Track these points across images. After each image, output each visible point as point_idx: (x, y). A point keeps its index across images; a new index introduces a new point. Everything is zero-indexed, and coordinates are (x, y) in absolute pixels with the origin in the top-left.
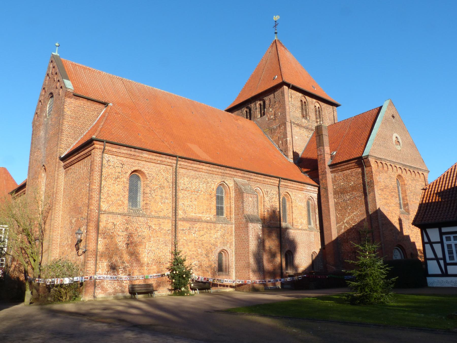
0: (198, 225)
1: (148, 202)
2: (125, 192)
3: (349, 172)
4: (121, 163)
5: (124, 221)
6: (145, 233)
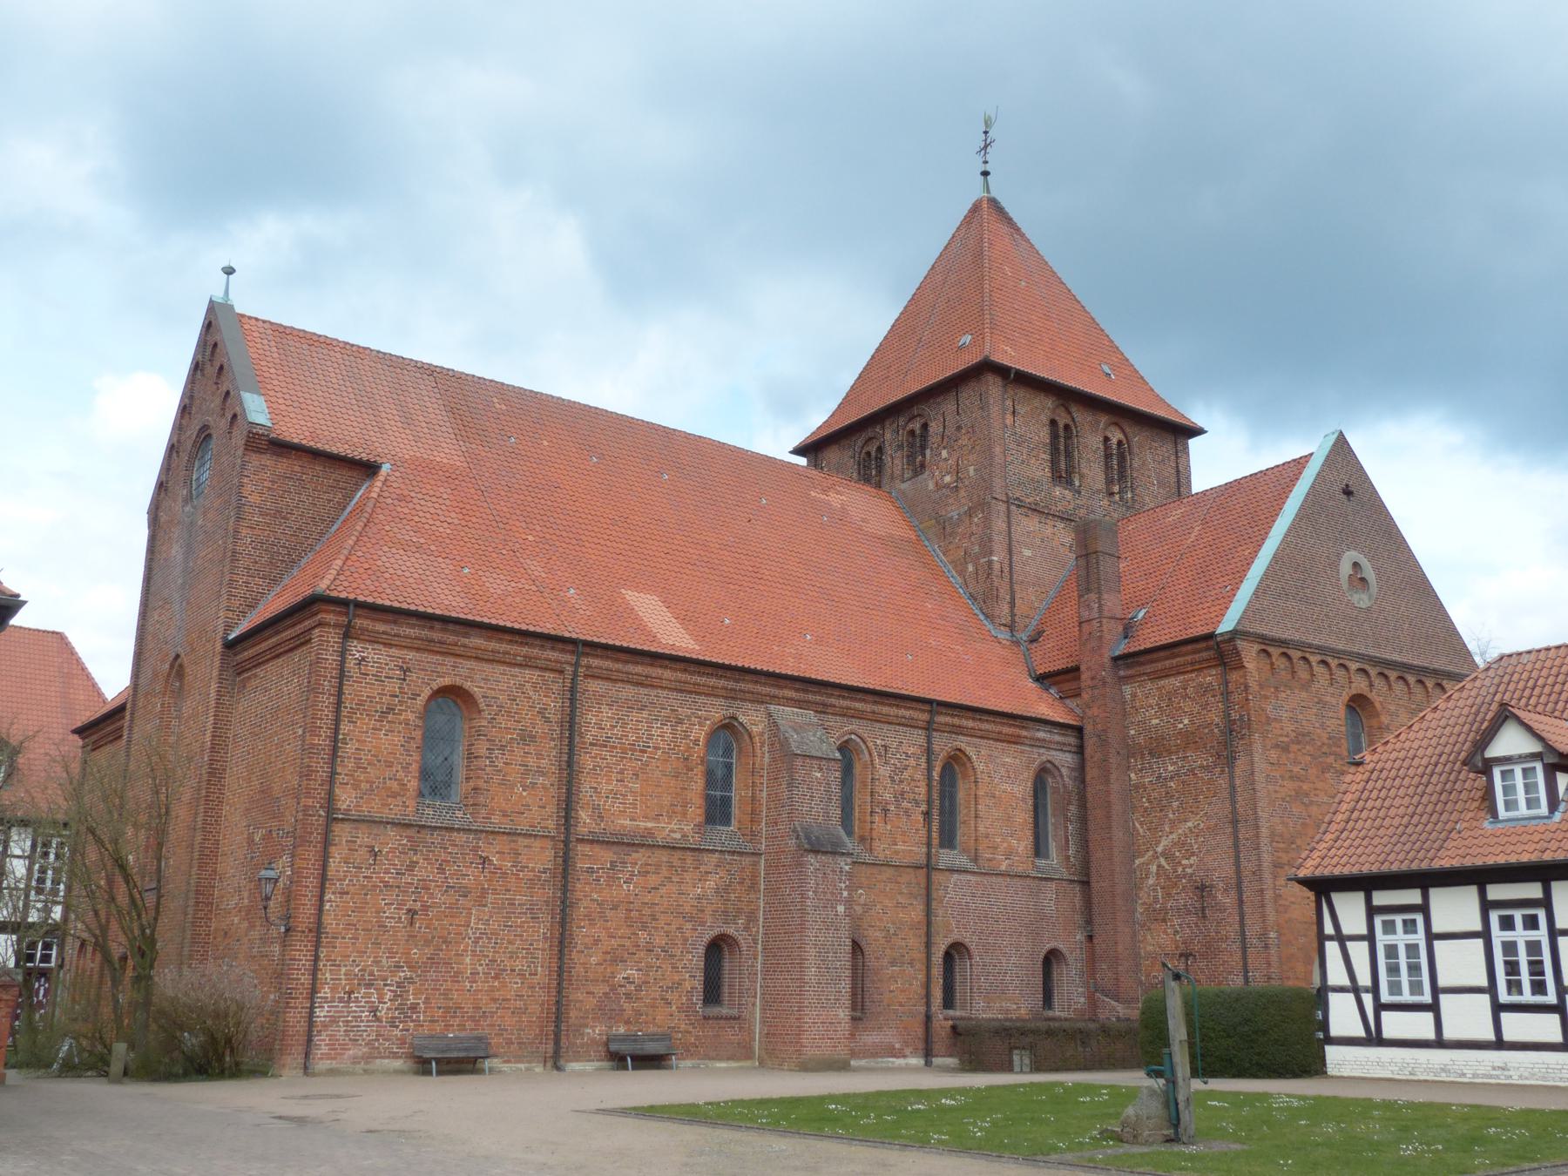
0: (640, 856)
1: (481, 783)
2: (411, 756)
3: (1175, 682)
4: (402, 667)
5: (405, 842)
6: (469, 880)
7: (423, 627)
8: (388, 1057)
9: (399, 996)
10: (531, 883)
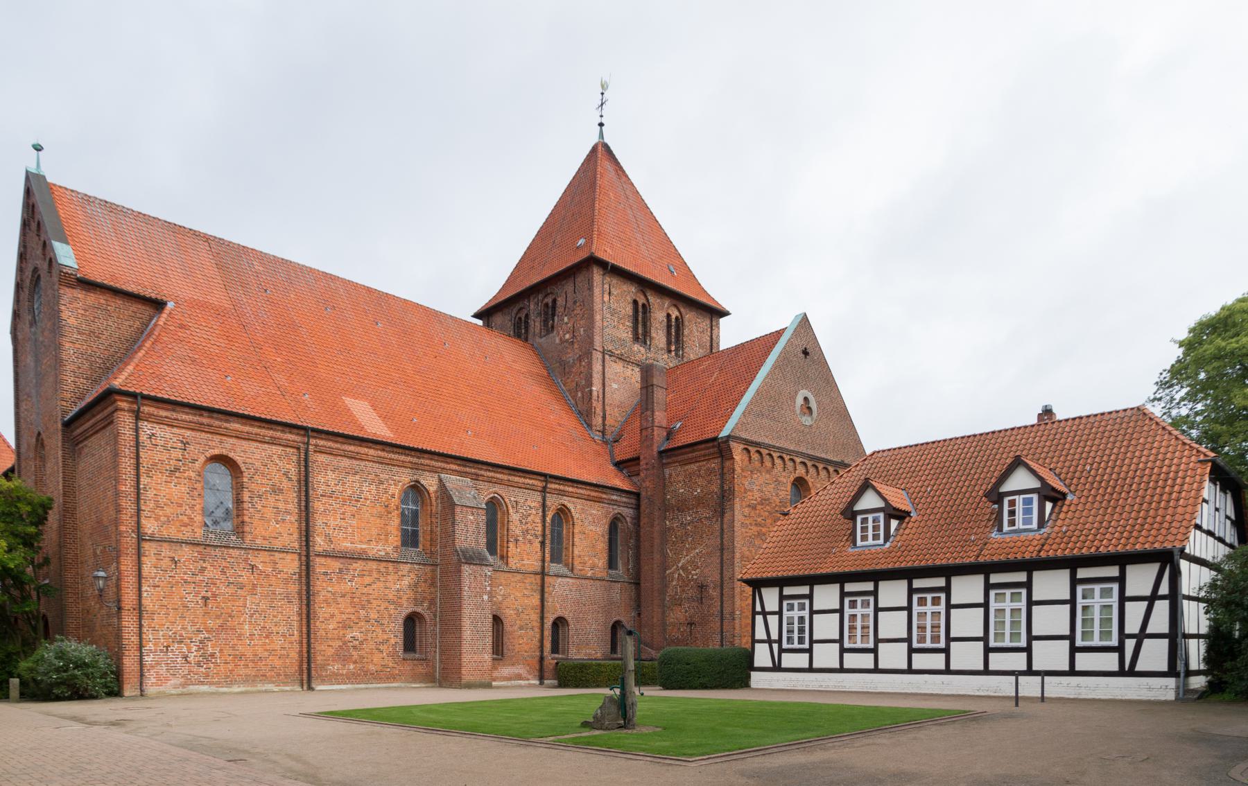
5: (196, 555)
7: (195, 415)
8: (197, 684)
9: (201, 648)
10: (286, 581)
